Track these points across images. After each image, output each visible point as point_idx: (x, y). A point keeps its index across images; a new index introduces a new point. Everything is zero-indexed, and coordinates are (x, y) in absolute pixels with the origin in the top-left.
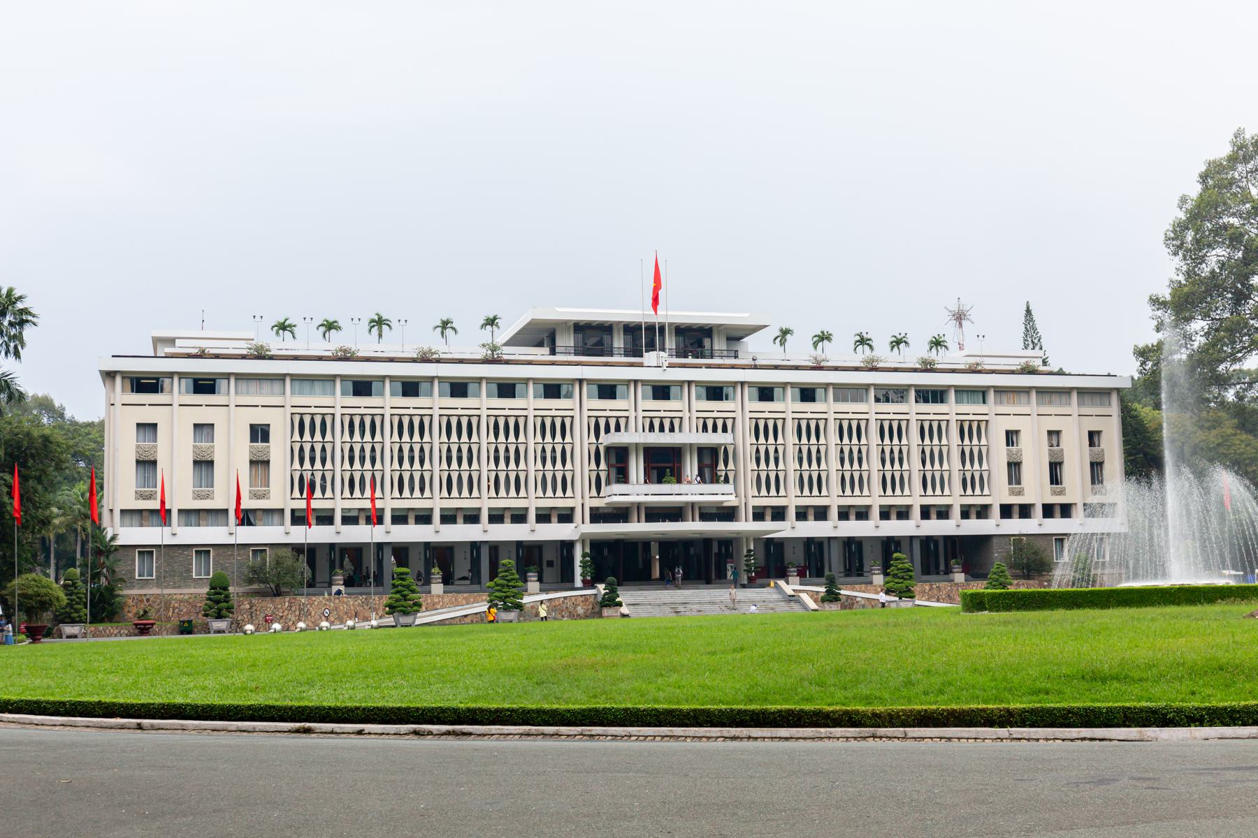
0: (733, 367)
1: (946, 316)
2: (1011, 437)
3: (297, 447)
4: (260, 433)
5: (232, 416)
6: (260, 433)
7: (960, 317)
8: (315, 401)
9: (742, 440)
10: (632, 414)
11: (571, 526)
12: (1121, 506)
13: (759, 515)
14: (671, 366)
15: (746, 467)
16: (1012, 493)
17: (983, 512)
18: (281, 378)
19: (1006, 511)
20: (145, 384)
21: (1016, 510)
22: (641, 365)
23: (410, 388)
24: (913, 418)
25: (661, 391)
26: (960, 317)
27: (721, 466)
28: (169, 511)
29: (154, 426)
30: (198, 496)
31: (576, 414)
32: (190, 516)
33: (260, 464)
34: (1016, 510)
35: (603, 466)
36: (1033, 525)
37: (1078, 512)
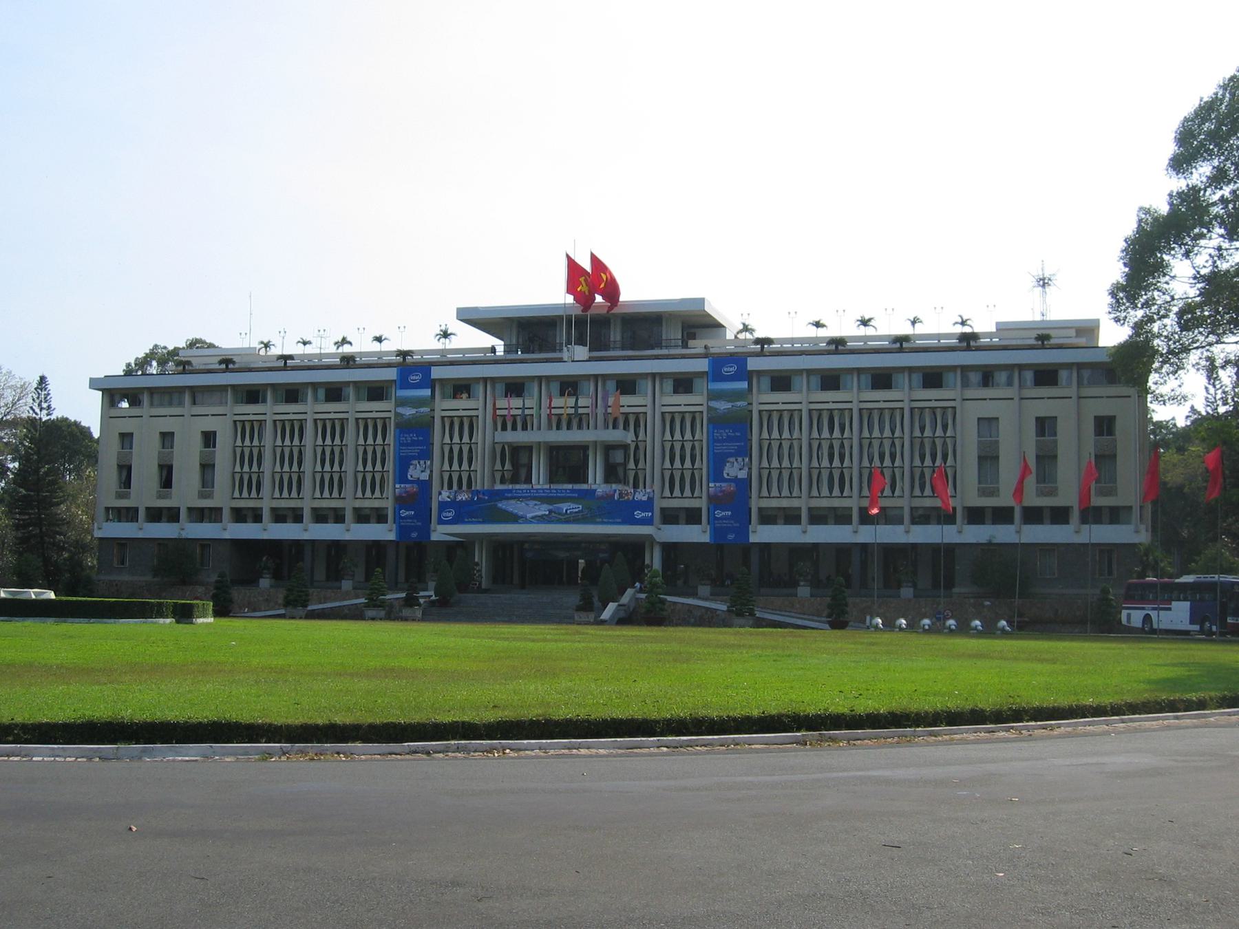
0: (684, 357)
1: (1031, 282)
2: (988, 423)
3: (239, 451)
4: (209, 439)
5: (189, 425)
6: (209, 439)
7: (1044, 282)
8: (250, 411)
9: (654, 437)
10: (649, 410)
11: (1011, 528)
12: (1136, 513)
13: (670, 517)
14: (590, 360)
15: (655, 465)
16: (983, 493)
17: (947, 518)
18: (222, 389)
19: (975, 516)
20: (134, 397)
21: (989, 515)
22: (560, 360)
23: (334, 393)
24: (269, 419)
25: (569, 386)
26: (1044, 282)
27: (631, 465)
28: (136, 510)
29: (132, 434)
30: (160, 497)
31: (480, 413)
32: (155, 515)
33: (207, 467)
34: (989, 515)
35: (508, 466)
36: (1003, 534)
37: (1075, 515)
